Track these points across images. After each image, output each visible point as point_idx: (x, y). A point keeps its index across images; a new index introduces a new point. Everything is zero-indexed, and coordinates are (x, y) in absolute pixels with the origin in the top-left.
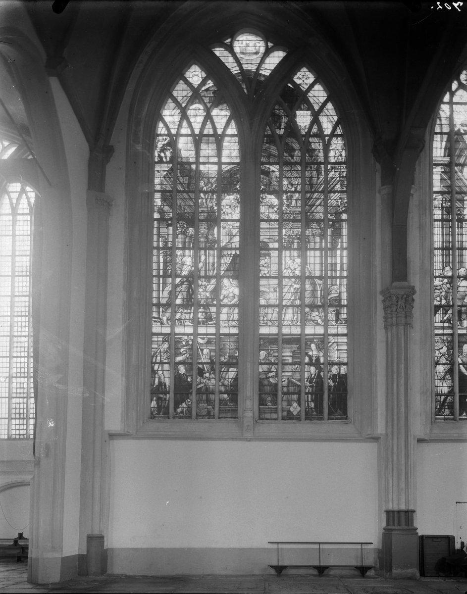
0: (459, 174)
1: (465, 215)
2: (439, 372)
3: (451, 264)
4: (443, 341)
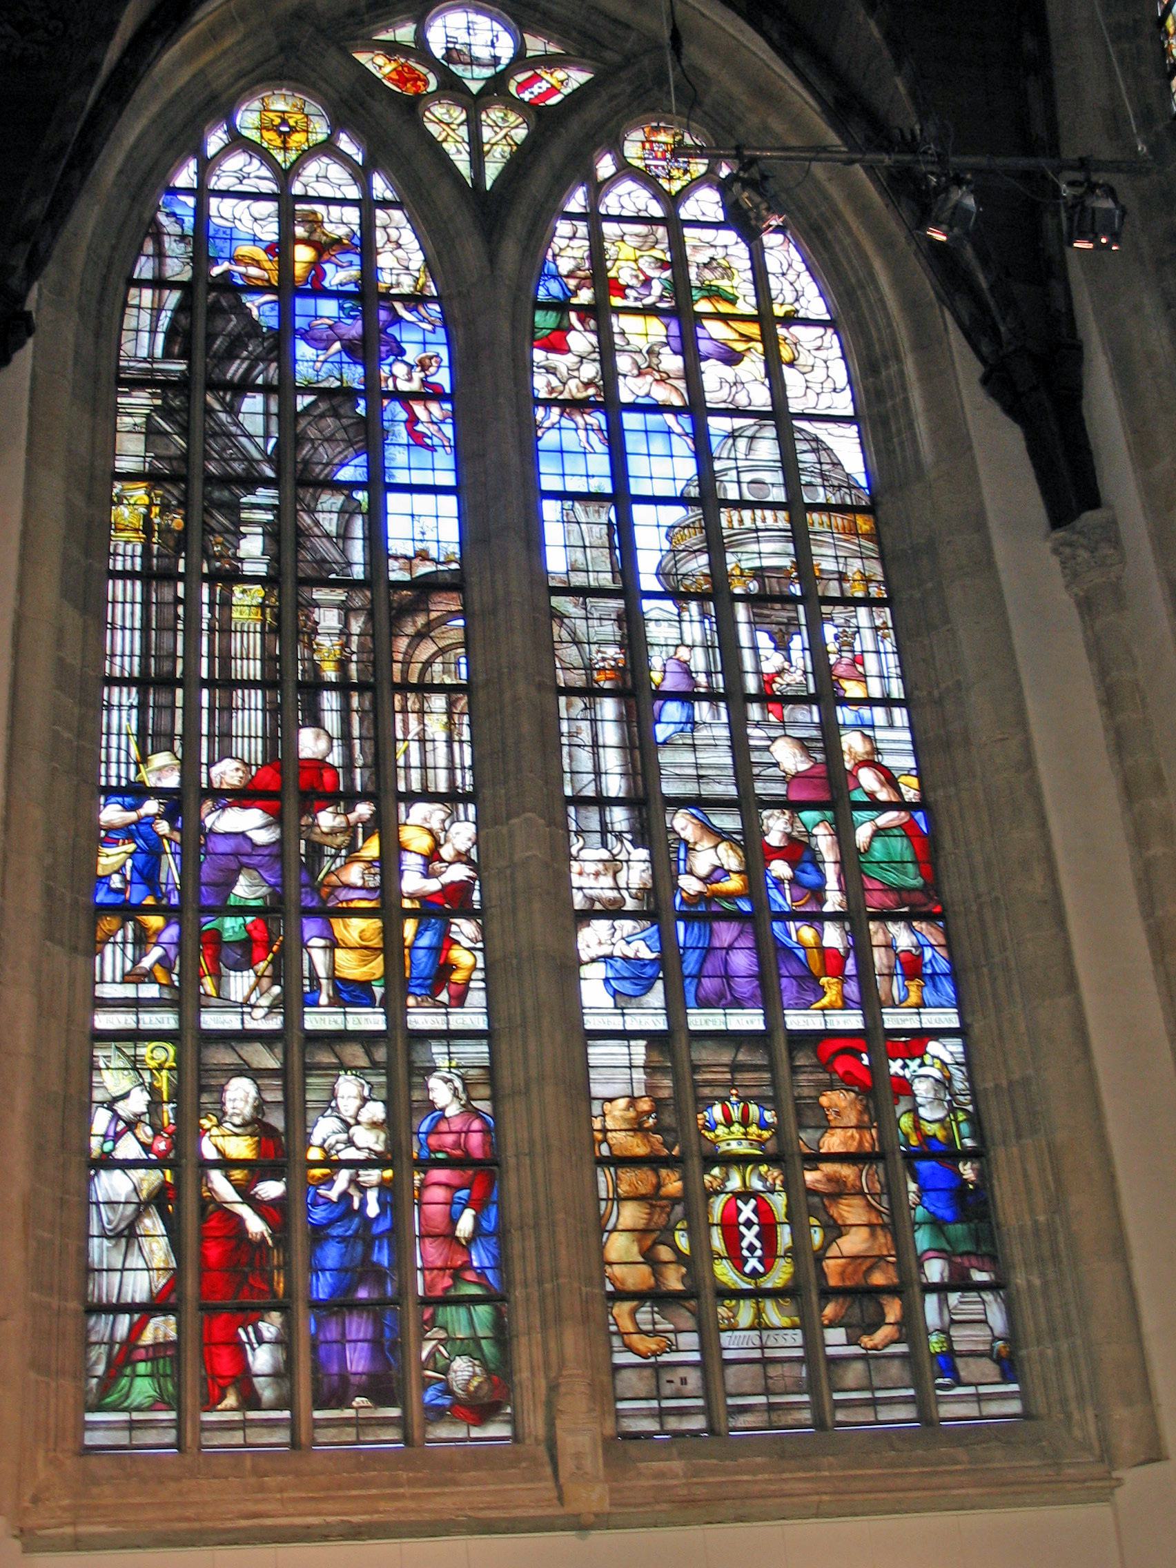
0: (223, 416)
1: (241, 560)
2: (109, 1203)
3: (177, 744)
4: (136, 1065)
